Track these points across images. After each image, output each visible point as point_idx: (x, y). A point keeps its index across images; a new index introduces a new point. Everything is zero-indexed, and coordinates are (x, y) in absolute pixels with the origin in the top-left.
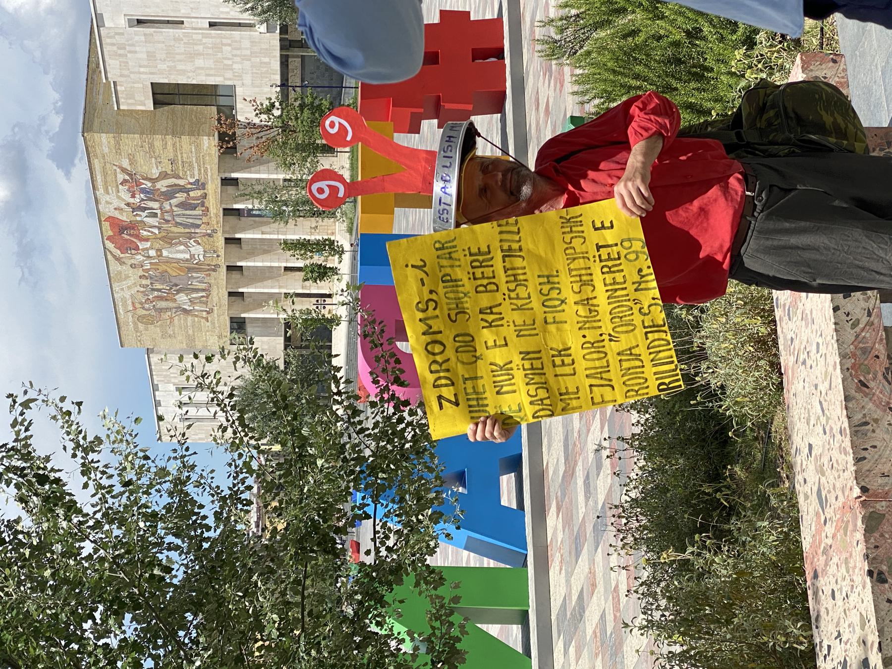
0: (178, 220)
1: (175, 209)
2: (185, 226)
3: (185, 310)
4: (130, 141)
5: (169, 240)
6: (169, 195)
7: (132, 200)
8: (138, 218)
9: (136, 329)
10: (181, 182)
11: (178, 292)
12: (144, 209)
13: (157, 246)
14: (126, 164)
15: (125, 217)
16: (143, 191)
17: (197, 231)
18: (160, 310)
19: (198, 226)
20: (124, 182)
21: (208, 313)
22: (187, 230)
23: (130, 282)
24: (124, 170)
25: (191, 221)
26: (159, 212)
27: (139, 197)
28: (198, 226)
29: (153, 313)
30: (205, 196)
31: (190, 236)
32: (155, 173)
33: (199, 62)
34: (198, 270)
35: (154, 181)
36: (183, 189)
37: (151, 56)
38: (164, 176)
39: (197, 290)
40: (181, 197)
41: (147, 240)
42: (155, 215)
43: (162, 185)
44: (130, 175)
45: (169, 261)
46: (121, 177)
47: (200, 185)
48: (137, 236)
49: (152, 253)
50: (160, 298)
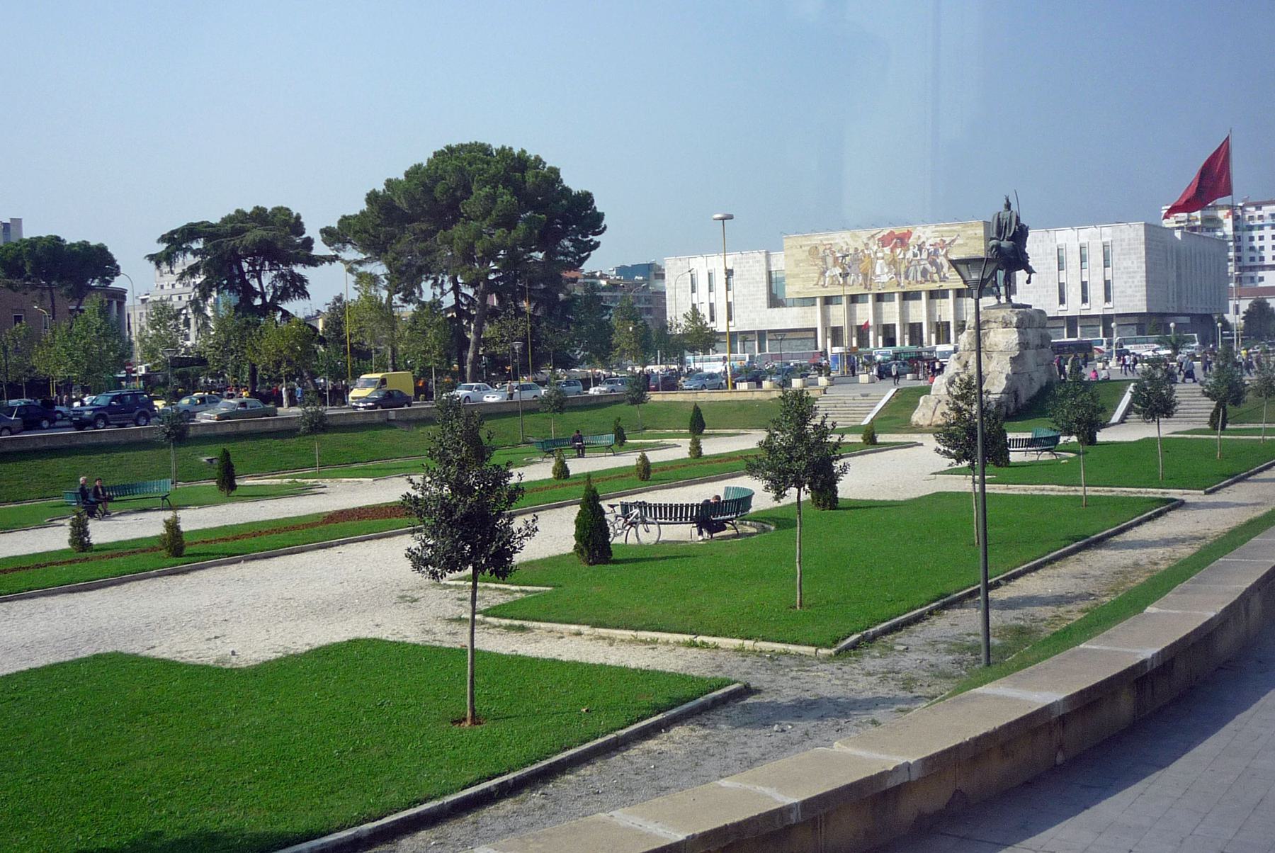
3: (823, 273)
5: (893, 263)
6: (933, 263)
10: (945, 269)
12: (920, 250)
16: (936, 250)
18: (824, 259)
21: (823, 286)
27: (932, 249)
28: (907, 278)
29: (821, 254)
30: (934, 281)
31: (898, 274)
41: (892, 251)
42: (915, 255)
45: (873, 264)
46: (948, 240)
47: (944, 279)
49: (880, 255)
50: (836, 259)
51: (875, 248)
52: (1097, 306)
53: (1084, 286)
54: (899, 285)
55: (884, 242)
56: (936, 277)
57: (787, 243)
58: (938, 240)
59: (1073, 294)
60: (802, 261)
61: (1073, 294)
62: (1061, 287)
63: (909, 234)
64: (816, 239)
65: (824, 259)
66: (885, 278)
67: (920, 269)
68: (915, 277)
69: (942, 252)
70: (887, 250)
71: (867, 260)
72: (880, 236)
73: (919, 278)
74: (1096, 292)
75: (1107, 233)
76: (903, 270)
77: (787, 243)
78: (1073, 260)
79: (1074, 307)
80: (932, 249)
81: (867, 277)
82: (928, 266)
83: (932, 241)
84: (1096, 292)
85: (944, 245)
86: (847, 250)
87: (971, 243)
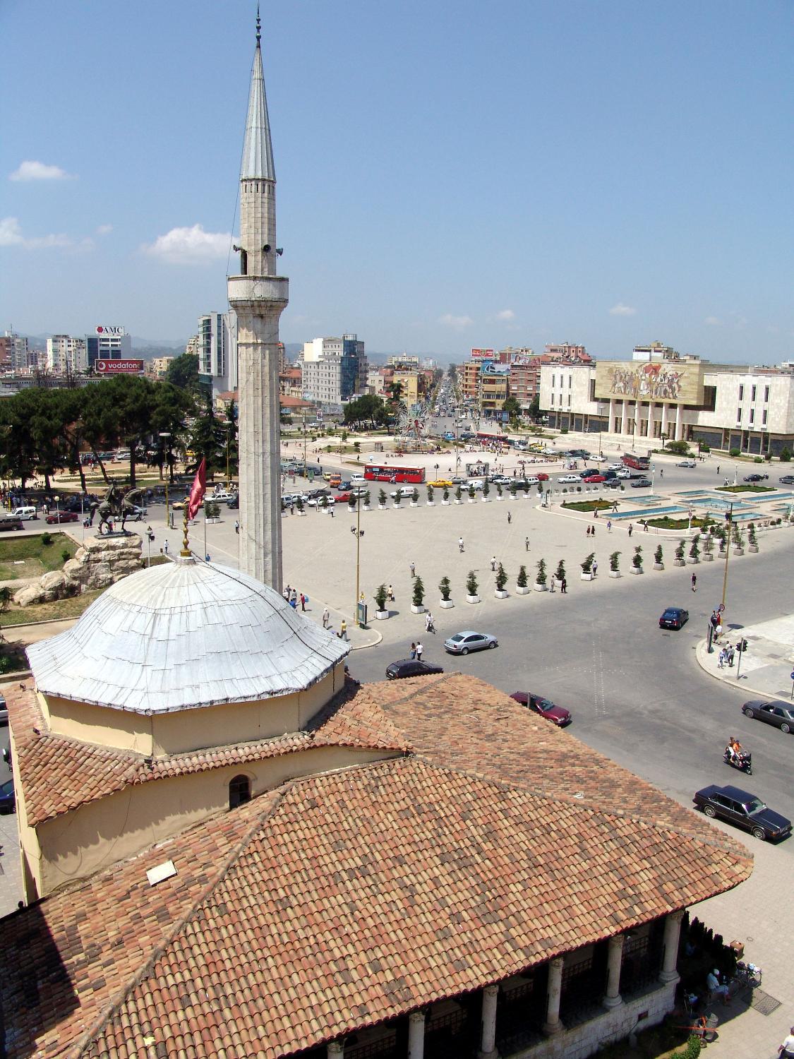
2: (656, 390)
4: (695, 379)
5: (650, 384)
6: (670, 387)
10: (676, 391)
12: (664, 378)
14: (685, 375)
16: (673, 379)
18: (615, 376)
19: (656, 393)
24: (682, 374)
28: (656, 393)
31: (651, 391)
32: (680, 384)
33: (725, 403)
34: (635, 391)
36: (673, 392)
37: (728, 389)
38: (679, 387)
39: (625, 389)
40: (670, 391)
43: (675, 385)
46: (679, 373)
47: (675, 397)
49: (643, 378)
50: (621, 377)
52: (758, 426)
59: (746, 415)
61: (746, 415)
63: (660, 367)
64: (612, 365)
65: (615, 376)
66: (645, 393)
67: (663, 389)
69: (676, 381)
70: (647, 375)
72: (644, 366)
74: (759, 417)
76: (654, 388)
78: (748, 393)
79: (745, 425)
81: (636, 390)
83: (671, 373)
84: (759, 417)
85: (677, 376)
87: (692, 377)
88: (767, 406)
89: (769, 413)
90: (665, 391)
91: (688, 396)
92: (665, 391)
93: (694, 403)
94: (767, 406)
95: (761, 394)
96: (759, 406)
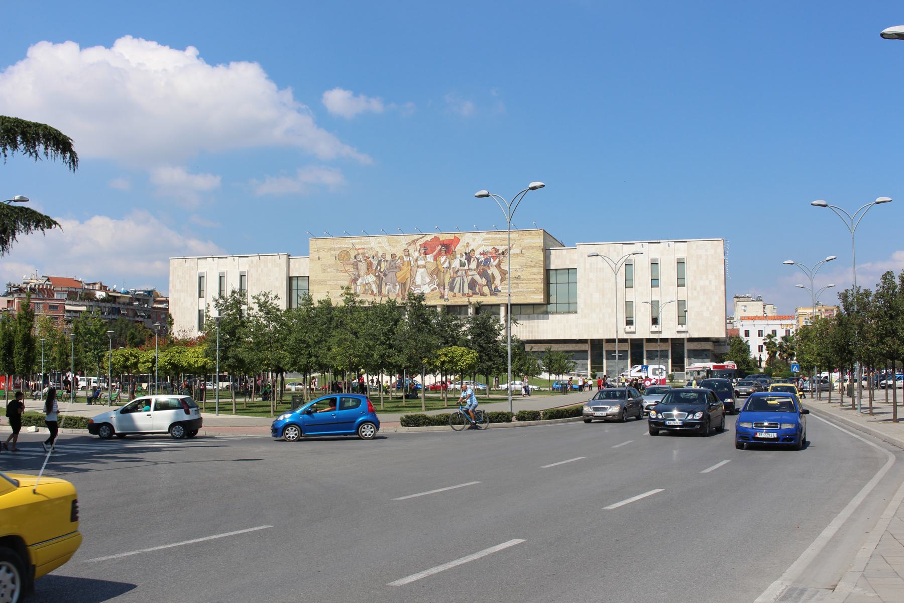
0: (458, 280)
1: (470, 278)
5: (436, 272)
6: (483, 274)
7: (477, 255)
8: (458, 256)
9: (334, 249)
10: (497, 281)
11: (378, 277)
13: (428, 266)
14: (512, 252)
15: (458, 247)
16: (487, 261)
17: (447, 290)
18: (356, 265)
19: (452, 289)
20: (497, 250)
22: (447, 284)
23: (387, 246)
25: (457, 286)
26: (466, 267)
27: (482, 258)
28: (452, 289)
29: (353, 260)
30: (483, 295)
31: (441, 285)
32: (504, 267)
35: (498, 266)
38: (503, 273)
39: (380, 287)
40: (484, 281)
41: (435, 259)
42: (462, 265)
44: (503, 253)
46: (501, 249)
47: (495, 292)
48: (439, 253)
49: (421, 262)
50: (370, 265)
51: (416, 255)
52: (669, 330)
53: (655, 305)
54: (442, 297)
55: (426, 249)
56: (486, 290)
57: (313, 245)
58: (490, 249)
60: (329, 266)
62: (629, 305)
64: (346, 243)
67: (467, 280)
68: (461, 289)
70: (430, 258)
71: (405, 268)
72: (422, 241)
73: (466, 290)
75: (681, 250)
76: (447, 280)
77: (313, 245)
78: (642, 274)
79: (643, 330)
80: (482, 258)
82: (477, 278)
86: (383, 256)
88: (683, 293)
89: (689, 305)
90: (473, 284)
91: (523, 287)
92: (473, 284)
93: (539, 298)
94: (683, 293)
95: (668, 274)
96: (668, 293)
